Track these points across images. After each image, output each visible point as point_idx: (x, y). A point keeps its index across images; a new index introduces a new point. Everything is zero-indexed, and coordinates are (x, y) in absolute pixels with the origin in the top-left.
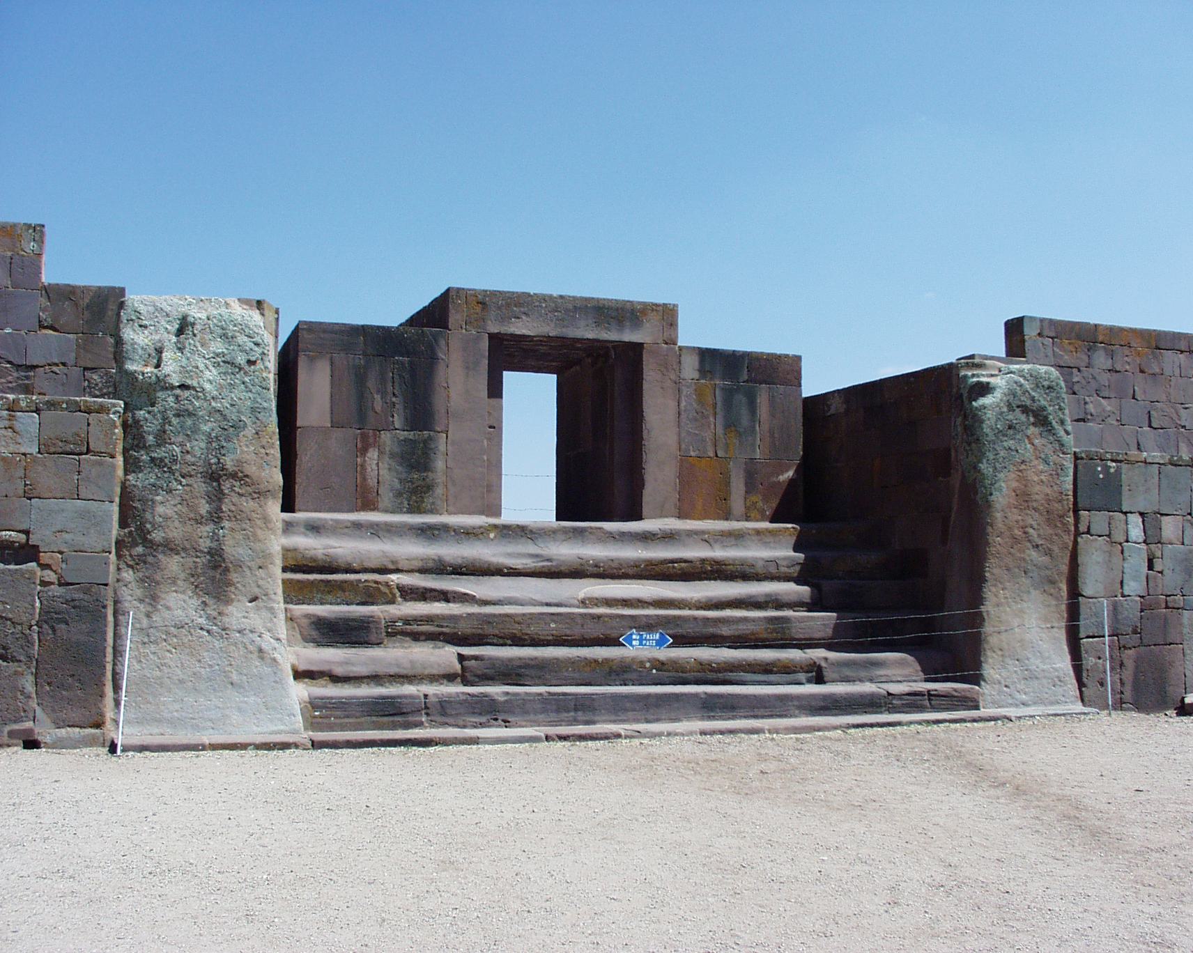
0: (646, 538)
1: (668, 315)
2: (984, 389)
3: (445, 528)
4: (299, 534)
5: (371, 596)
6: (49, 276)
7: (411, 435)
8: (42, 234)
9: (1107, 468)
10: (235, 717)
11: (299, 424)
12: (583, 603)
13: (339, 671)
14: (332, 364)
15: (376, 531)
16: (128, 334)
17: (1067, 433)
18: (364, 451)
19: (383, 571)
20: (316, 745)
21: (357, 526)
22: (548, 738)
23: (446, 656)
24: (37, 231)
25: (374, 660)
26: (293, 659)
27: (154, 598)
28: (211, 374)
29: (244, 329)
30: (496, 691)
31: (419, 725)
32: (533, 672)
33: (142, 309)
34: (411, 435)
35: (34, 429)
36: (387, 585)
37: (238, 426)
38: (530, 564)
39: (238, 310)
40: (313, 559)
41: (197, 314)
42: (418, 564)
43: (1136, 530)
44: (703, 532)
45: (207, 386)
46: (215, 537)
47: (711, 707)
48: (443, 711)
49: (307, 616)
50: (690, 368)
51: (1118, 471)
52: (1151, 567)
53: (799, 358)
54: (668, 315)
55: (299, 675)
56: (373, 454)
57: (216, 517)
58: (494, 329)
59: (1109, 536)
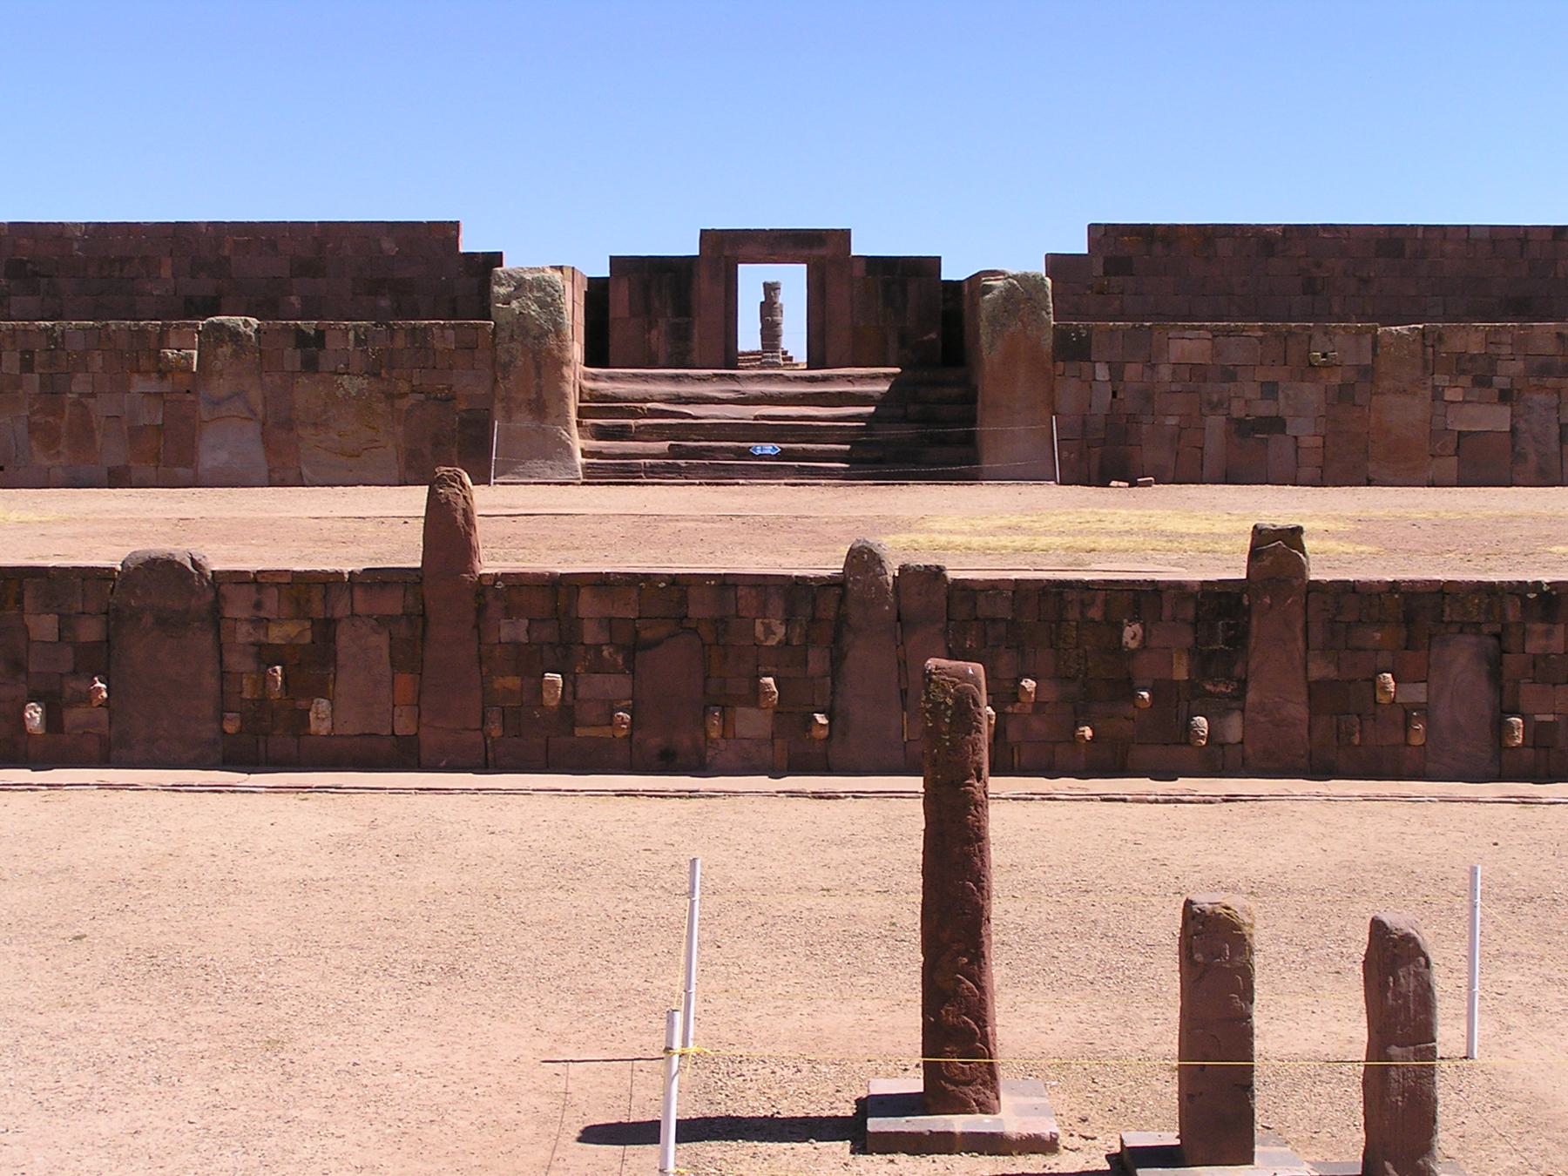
0: (825, 379)
1: (845, 235)
2: (990, 289)
3: (687, 376)
4: (603, 381)
5: (633, 414)
6: (464, 248)
7: (677, 320)
8: (458, 226)
9: (1078, 335)
10: (549, 471)
11: (611, 316)
12: (756, 418)
13: (605, 451)
14: (629, 279)
15: (646, 379)
16: (496, 289)
17: (1048, 313)
18: (649, 332)
19: (645, 401)
20: (583, 484)
21: (635, 375)
22: (700, 484)
23: (665, 445)
24: (455, 225)
25: (626, 447)
26: (583, 446)
27: (510, 417)
28: (535, 307)
29: (551, 284)
30: (681, 462)
31: (641, 477)
32: (711, 454)
33: (502, 275)
34: (677, 320)
35: (453, 338)
36: (641, 408)
37: (546, 333)
38: (732, 395)
39: (549, 270)
40: (606, 396)
41: (528, 277)
42: (664, 397)
43: (1102, 372)
44: (849, 376)
45: (533, 313)
46: (538, 385)
47: (801, 472)
48: (652, 471)
49: (593, 425)
50: (859, 271)
51: (1089, 337)
52: (1114, 395)
53: (939, 258)
54: (845, 235)
55: (585, 454)
56: (654, 333)
57: (539, 375)
58: (727, 253)
59: (1080, 377)
